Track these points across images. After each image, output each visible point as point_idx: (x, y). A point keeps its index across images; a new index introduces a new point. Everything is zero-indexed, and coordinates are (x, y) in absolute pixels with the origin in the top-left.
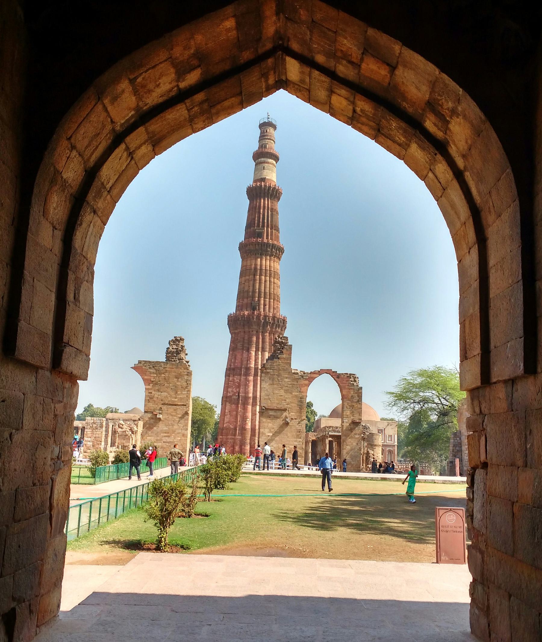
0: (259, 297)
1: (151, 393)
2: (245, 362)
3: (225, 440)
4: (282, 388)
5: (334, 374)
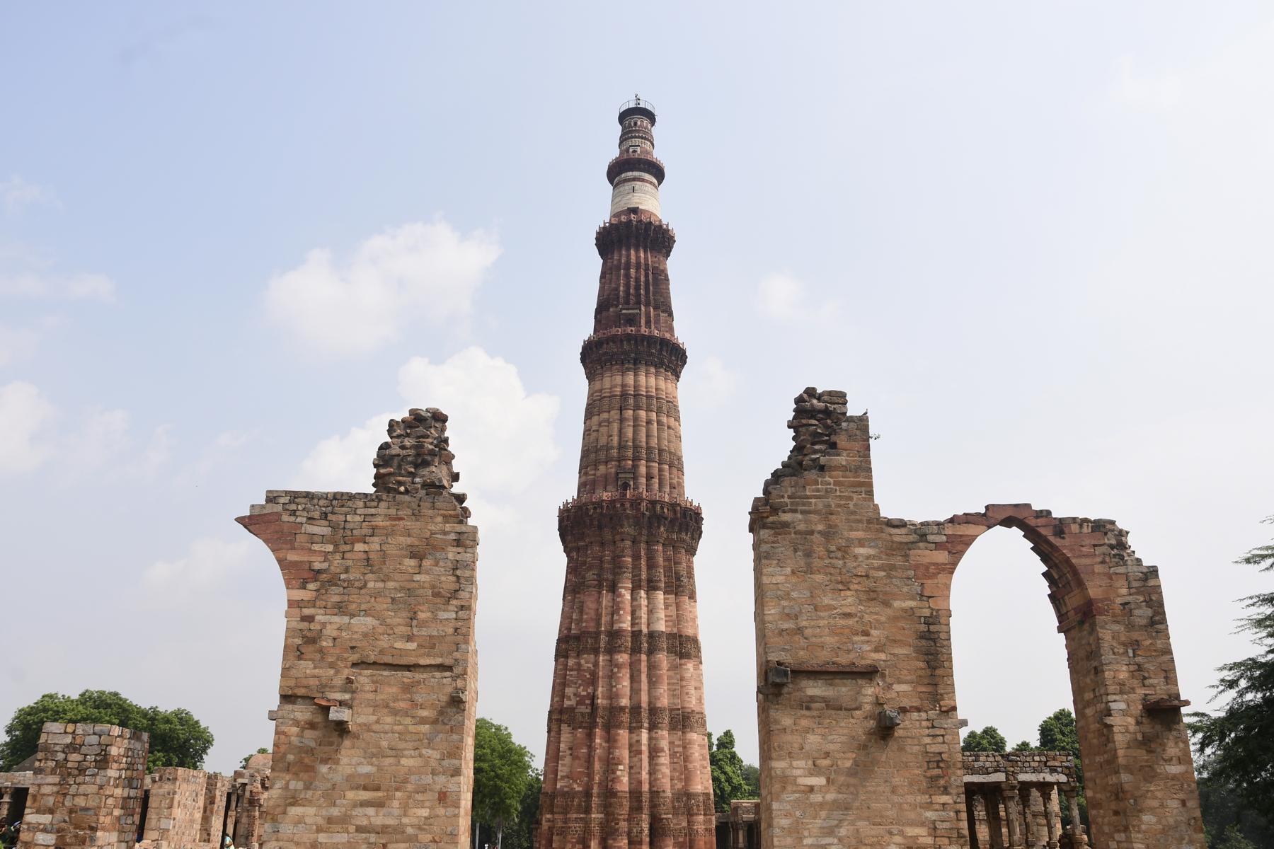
0: (636, 459)
1: (310, 619)
2: (605, 619)
3: (560, 824)
4: (846, 585)
5: (1041, 521)
